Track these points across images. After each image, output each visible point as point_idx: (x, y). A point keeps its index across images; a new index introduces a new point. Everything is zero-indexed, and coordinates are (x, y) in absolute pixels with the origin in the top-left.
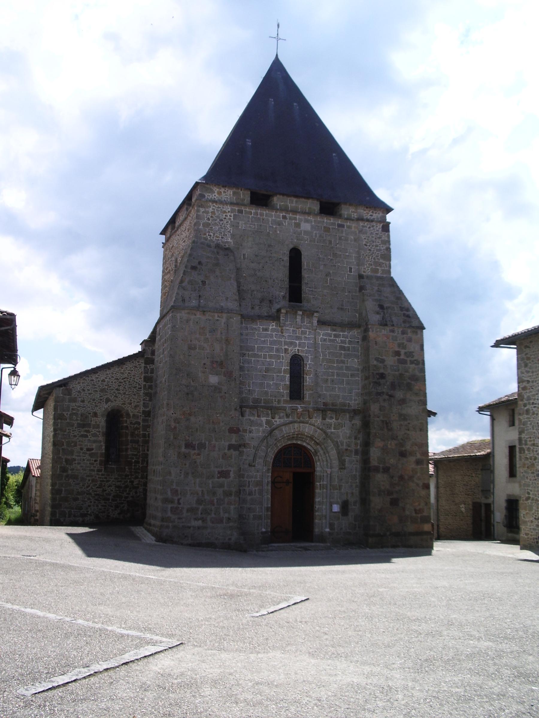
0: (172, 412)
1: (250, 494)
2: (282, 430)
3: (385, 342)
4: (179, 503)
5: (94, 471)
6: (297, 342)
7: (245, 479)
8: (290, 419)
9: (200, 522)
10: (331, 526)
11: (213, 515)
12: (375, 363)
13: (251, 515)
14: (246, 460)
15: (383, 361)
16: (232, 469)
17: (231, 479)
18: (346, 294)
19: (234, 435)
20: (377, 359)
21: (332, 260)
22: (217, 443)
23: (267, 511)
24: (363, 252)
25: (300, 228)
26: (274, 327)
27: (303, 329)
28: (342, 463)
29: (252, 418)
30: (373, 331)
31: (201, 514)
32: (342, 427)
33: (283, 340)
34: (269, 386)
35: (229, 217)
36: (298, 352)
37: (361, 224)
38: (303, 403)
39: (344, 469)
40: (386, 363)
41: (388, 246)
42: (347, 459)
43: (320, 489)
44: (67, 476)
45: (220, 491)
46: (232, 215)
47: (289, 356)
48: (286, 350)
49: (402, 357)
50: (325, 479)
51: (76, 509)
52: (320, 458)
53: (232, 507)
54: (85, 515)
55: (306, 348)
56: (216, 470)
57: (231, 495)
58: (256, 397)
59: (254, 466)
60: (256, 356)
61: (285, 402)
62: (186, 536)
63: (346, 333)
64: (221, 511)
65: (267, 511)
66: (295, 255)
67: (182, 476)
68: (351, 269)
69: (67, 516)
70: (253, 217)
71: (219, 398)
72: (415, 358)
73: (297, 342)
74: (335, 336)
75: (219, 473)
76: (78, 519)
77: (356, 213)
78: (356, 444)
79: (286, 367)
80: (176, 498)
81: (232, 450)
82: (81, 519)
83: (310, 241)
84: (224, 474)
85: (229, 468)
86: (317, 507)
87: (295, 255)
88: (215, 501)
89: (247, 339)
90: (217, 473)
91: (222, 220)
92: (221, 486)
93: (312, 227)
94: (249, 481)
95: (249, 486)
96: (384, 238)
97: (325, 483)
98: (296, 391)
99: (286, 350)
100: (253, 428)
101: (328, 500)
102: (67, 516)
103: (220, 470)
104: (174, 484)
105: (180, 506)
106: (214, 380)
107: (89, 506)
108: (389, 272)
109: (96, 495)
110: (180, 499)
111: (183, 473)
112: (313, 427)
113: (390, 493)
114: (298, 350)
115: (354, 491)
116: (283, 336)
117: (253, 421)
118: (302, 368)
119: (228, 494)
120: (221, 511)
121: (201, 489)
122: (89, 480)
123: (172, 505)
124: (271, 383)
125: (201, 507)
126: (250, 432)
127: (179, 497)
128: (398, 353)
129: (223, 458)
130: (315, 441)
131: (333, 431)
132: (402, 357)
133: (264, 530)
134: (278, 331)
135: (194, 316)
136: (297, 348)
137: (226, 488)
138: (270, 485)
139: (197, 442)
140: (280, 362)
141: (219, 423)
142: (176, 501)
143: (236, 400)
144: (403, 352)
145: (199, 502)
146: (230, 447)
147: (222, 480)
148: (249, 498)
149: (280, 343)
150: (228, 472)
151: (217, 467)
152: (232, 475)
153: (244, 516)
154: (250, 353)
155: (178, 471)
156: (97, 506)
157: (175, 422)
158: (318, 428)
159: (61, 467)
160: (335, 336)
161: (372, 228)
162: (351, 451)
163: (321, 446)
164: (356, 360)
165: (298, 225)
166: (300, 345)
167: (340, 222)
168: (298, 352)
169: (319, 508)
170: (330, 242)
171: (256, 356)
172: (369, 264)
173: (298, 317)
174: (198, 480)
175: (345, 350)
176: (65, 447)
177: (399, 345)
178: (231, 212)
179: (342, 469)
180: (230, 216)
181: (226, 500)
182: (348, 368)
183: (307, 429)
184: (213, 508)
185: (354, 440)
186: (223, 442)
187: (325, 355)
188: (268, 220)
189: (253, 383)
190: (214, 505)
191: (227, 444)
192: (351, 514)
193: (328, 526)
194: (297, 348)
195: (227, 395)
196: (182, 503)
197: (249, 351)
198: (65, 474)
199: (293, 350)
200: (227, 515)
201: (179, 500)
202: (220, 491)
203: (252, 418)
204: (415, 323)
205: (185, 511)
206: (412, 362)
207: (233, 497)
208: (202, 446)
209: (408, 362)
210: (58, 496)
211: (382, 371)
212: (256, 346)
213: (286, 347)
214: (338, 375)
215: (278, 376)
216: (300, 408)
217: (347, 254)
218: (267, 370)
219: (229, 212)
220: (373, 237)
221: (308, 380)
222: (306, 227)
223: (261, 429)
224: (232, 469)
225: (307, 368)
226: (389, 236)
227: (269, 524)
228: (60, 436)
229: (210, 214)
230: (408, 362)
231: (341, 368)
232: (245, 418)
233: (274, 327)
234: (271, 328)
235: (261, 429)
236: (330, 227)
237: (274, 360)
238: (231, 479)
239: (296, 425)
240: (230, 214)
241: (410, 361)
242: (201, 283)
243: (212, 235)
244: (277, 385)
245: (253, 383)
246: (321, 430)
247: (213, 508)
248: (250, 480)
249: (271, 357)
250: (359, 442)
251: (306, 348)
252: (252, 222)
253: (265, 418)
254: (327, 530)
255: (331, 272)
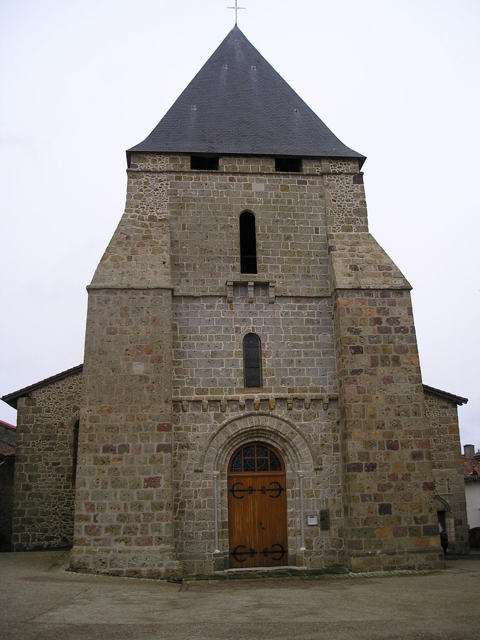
0: (88, 409)
1: (198, 506)
2: (235, 425)
3: (360, 309)
4: (96, 521)
5: (60, 487)
6: (251, 318)
7: (191, 488)
8: (247, 412)
9: (123, 543)
10: (308, 543)
11: (139, 535)
12: (348, 334)
13: (200, 533)
14: (190, 464)
15: (358, 332)
16: (163, 476)
17: (161, 488)
18: (313, 259)
19: (165, 433)
20: (350, 330)
21: (293, 221)
22: (143, 444)
23: (223, 528)
24: (330, 209)
25: (251, 190)
26: (221, 303)
27: (258, 303)
28: (318, 461)
29: (196, 413)
30: (343, 296)
31: (124, 533)
32: (315, 417)
33: (233, 317)
34: (217, 373)
35: (165, 185)
36: (253, 330)
37: (326, 178)
38: (263, 391)
39: (321, 469)
40: (362, 334)
41: (361, 199)
42: (324, 457)
43: (293, 497)
44: (30, 495)
45: (147, 504)
46: (169, 183)
47: (241, 337)
48: (237, 329)
49: (384, 324)
50: (297, 484)
51: (41, 532)
52: (289, 458)
53: (164, 524)
54: (49, 539)
55: (263, 325)
56: (143, 477)
57: (161, 508)
58: (201, 387)
59: (201, 471)
60: (198, 338)
61: (239, 391)
62: (103, 563)
63: (314, 304)
64: (150, 529)
65: (223, 528)
66: (247, 221)
67: (100, 487)
68: (317, 229)
69: (31, 539)
70: (194, 183)
71: (145, 389)
72: (401, 325)
73: (251, 318)
74: (300, 307)
75: (146, 480)
76: (43, 542)
77: (320, 166)
78: (335, 438)
79: (237, 347)
80: (92, 515)
81: (162, 452)
82: (46, 543)
83: (265, 202)
84: (152, 482)
85: (159, 475)
86: (290, 519)
87: (247, 221)
88: (142, 516)
89: (188, 320)
90: (143, 481)
91: (157, 190)
92: (149, 497)
93: (266, 187)
94: (196, 491)
95: (195, 497)
96: (357, 190)
97: (297, 489)
98: (253, 377)
99: (237, 329)
100: (198, 425)
101: (302, 511)
102: (31, 539)
103: (147, 477)
104: (90, 497)
105: (96, 524)
106: (139, 368)
107: (56, 528)
108: (366, 229)
109: (63, 514)
110: (97, 515)
111: (100, 483)
112: (277, 420)
113: (376, 498)
114: (253, 328)
115: (336, 497)
116: (233, 313)
117: (198, 416)
118: (259, 348)
119: (158, 507)
120: (150, 529)
121: (123, 502)
122: (55, 499)
123: (87, 524)
124: (220, 369)
125: (123, 525)
126: (195, 430)
127: (96, 513)
128: (378, 321)
129: (151, 462)
130: (281, 438)
131: (303, 423)
132: (384, 324)
133: (217, 551)
134: (226, 307)
135: (115, 296)
136: (251, 326)
137: (155, 500)
138: (226, 494)
139: (118, 445)
140: (231, 343)
141: (146, 419)
142: (92, 519)
143: (166, 390)
144: (384, 319)
145: (122, 518)
146: (160, 448)
147: (150, 489)
148: (196, 511)
149: (228, 321)
150: (158, 479)
151: (142, 474)
152: (162, 482)
153: (191, 535)
154: (192, 335)
155: (94, 481)
156: (65, 528)
157: (90, 421)
158: (283, 420)
159: (24, 485)
160: (300, 307)
161: (341, 181)
162: (329, 447)
163: (289, 443)
164: (329, 335)
165: (249, 187)
166: (254, 321)
167: (300, 179)
168: (253, 330)
169: (291, 521)
170: (290, 202)
171: (198, 338)
172: (340, 221)
173: (249, 289)
174: (119, 490)
175: (313, 324)
176: (28, 462)
177: (379, 310)
178: (168, 180)
179: (318, 469)
180: (167, 184)
181: (156, 513)
182: (318, 345)
183: (269, 423)
184: (139, 525)
185: (331, 433)
186: (151, 442)
187: (287, 332)
188: (211, 184)
189: (196, 370)
190: (140, 522)
191: (156, 444)
192: (333, 527)
193: (303, 544)
194: (251, 326)
195: (155, 386)
196: (99, 520)
197: (191, 333)
198: (28, 493)
199: (246, 329)
200: (156, 534)
201: (95, 517)
202: (147, 504)
203: (196, 413)
204: (399, 283)
205: (103, 530)
206: (397, 331)
207: (164, 511)
208: (124, 448)
209: (393, 331)
210: (20, 518)
211: (358, 344)
212: (199, 327)
213: (237, 325)
214: (306, 354)
215: (228, 360)
216: (257, 396)
217: (312, 213)
218: (214, 354)
219: (165, 180)
220: (342, 191)
221: (267, 363)
222: (258, 186)
223: (208, 425)
224: (163, 476)
225: (265, 349)
226: (363, 189)
227: (227, 543)
228: (23, 451)
229: (143, 185)
230: (393, 331)
231: (310, 346)
232: (187, 413)
233: (221, 303)
234: (217, 304)
235: (208, 425)
236: (289, 185)
237: (222, 342)
238: (161, 488)
239: (254, 419)
240: (166, 182)
241: (395, 329)
242: (126, 259)
243: (145, 206)
244: (228, 372)
245: (196, 370)
246: (287, 422)
247: (139, 525)
248: (197, 489)
249: (218, 338)
250: (338, 435)
251: (263, 325)
252: (193, 188)
253: (213, 412)
254: (303, 549)
255: (292, 235)
